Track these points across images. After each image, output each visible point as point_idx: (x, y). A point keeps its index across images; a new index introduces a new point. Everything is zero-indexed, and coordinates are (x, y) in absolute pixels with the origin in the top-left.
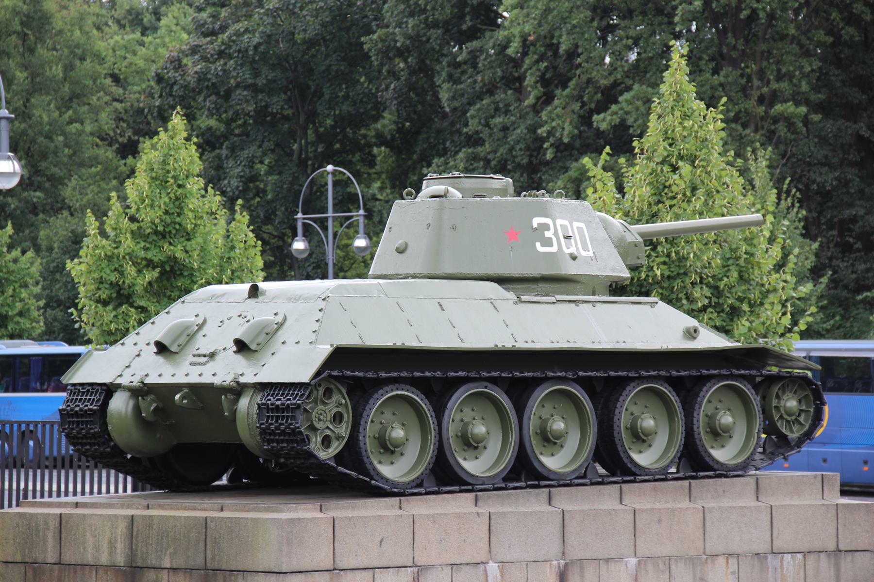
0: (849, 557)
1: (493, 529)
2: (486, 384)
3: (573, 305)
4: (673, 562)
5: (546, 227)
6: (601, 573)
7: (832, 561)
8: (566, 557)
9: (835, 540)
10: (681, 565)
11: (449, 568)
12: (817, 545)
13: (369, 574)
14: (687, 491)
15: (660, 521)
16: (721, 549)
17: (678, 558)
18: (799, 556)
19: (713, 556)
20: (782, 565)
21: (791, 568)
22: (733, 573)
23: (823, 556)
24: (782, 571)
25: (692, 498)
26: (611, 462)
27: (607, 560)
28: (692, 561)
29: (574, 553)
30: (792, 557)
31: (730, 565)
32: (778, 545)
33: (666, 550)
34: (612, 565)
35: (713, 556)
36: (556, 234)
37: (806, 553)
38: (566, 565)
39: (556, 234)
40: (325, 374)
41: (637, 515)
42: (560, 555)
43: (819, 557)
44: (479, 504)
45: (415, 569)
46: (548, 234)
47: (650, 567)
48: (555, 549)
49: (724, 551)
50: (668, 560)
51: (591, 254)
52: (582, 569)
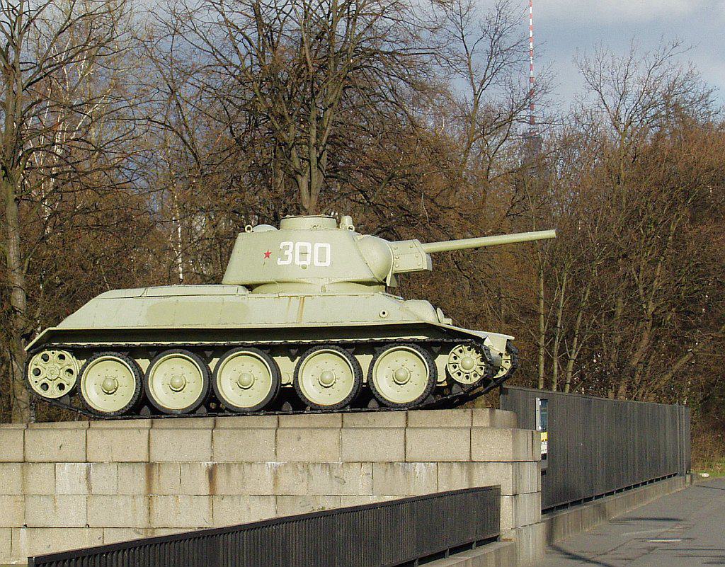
0: (482, 466)
2: (181, 350)
5: (287, 247)
10: (318, 468)
14: (340, 419)
15: (299, 439)
21: (424, 471)
22: (367, 474)
23: (454, 464)
26: (287, 400)
27: (251, 463)
29: (222, 458)
33: (305, 457)
34: (255, 466)
36: (293, 253)
38: (215, 466)
39: (293, 253)
46: (286, 252)
47: (289, 468)
49: (359, 460)
50: (306, 465)
51: (328, 264)
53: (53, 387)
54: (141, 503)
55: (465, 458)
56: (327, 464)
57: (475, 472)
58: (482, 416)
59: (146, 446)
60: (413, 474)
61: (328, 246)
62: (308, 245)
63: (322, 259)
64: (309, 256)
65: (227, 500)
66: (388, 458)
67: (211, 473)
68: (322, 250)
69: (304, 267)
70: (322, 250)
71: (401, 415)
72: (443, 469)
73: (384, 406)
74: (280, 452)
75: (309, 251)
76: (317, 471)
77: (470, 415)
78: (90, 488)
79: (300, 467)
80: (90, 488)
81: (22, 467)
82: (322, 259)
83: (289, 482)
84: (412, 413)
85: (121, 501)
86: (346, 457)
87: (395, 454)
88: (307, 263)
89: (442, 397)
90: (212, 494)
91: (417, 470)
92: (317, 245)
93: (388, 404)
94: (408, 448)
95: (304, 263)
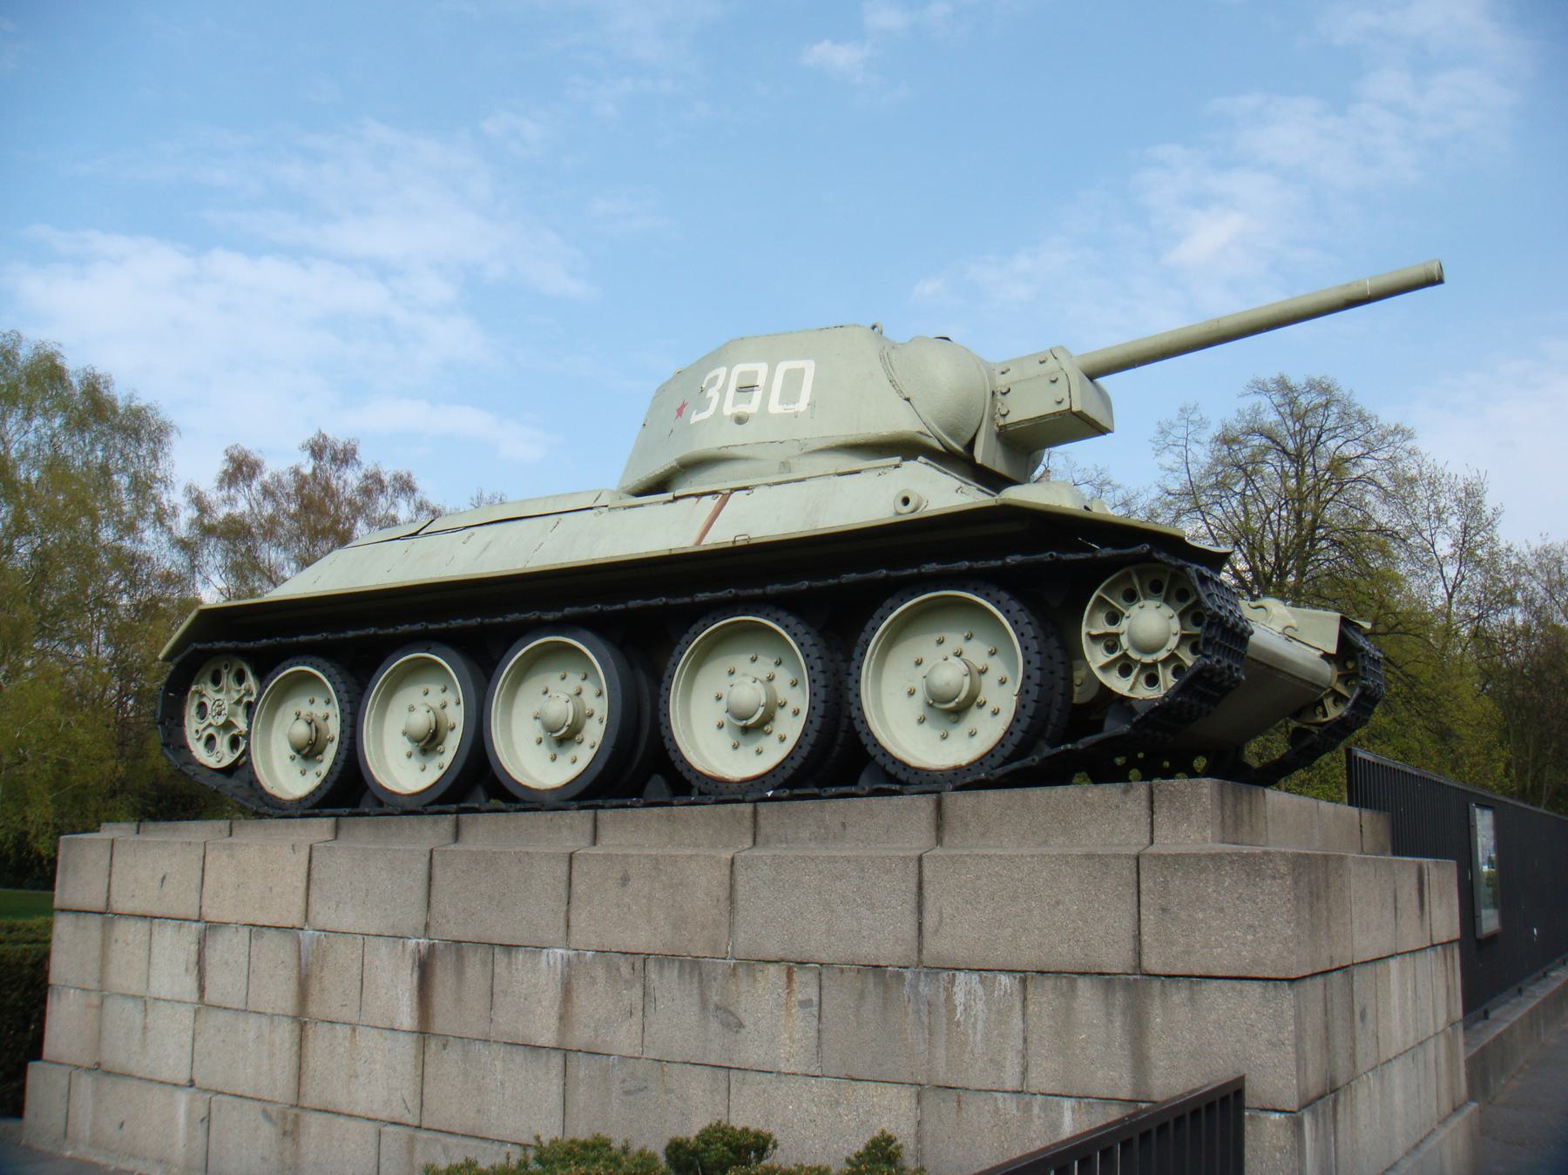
0: (1179, 994)
1: (315, 876)
3: (694, 500)
4: (651, 964)
6: (497, 970)
7: (1119, 998)
8: (432, 933)
9: (1130, 945)
10: (672, 973)
11: (246, 930)
12: (1066, 955)
13: (143, 926)
14: (748, 823)
15: (625, 880)
16: (773, 949)
17: (665, 959)
18: (1004, 979)
19: (754, 963)
20: (949, 998)
22: (805, 1004)
23: (1083, 984)
24: (952, 1010)
25: (759, 839)
27: (509, 948)
28: (692, 966)
30: (982, 982)
31: (795, 986)
32: (938, 946)
33: (641, 939)
34: (520, 956)
35: (754, 963)
37: (1025, 977)
38: (431, 949)
40: (190, 649)
41: (575, 865)
42: (422, 928)
43: (1073, 988)
44: (341, 835)
45: (201, 925)
48: (416, 917)
49: (781, 954)
51: (802, 406)
52: (460, 958)
53: (223, 742)
54: (285, 1033)
55: (1116, 958)
56: (696, 962)
57: (1157, 1019)
58: (1191, 814)
59: (302, 885)
60: (943, 1011)
61: (809, 367)
62: (762, 368)
63: (790, 394)
64: (757, 396)
65: (454, 1054)
66: (868, 951)
67: (425, 968)
68: (794, 379)
69: (740, 420)
70: (794, 379)
71: (923, 805)
72: (1044, 997)
73: (897, 779)
74: (580, 918)
75: (761, 381)
76: (669, 986)
77: (1145, 803)
78: (202, 989)
79: (625, 970)
80: (202, 989)
81: (103, 925)
82: (790, 394)
83: (601, 1011)
84: (962, 803)
85: (251, 1026)
86: (744, 942)
87: (886, 938)
88: (751, 406)
89: (1063, 742)
90: (424, 1030)
91: (959, 998)
92: (783, 367)
93: (902, 776)
94: (930, 921)
95: (743, 409)
